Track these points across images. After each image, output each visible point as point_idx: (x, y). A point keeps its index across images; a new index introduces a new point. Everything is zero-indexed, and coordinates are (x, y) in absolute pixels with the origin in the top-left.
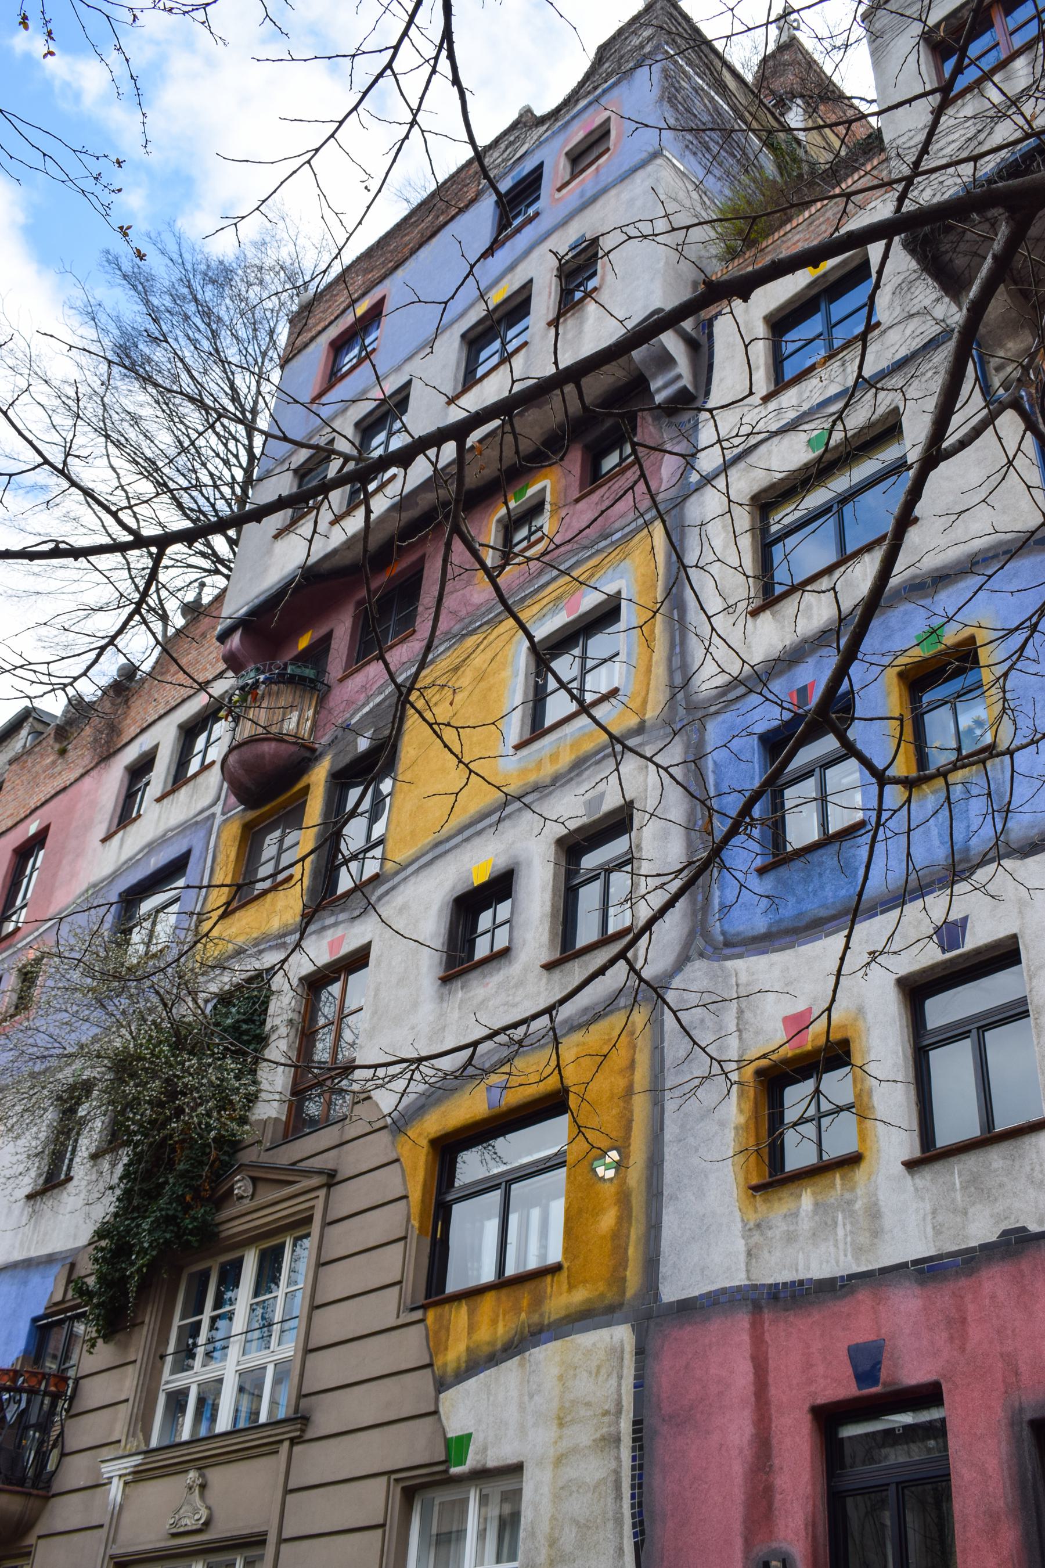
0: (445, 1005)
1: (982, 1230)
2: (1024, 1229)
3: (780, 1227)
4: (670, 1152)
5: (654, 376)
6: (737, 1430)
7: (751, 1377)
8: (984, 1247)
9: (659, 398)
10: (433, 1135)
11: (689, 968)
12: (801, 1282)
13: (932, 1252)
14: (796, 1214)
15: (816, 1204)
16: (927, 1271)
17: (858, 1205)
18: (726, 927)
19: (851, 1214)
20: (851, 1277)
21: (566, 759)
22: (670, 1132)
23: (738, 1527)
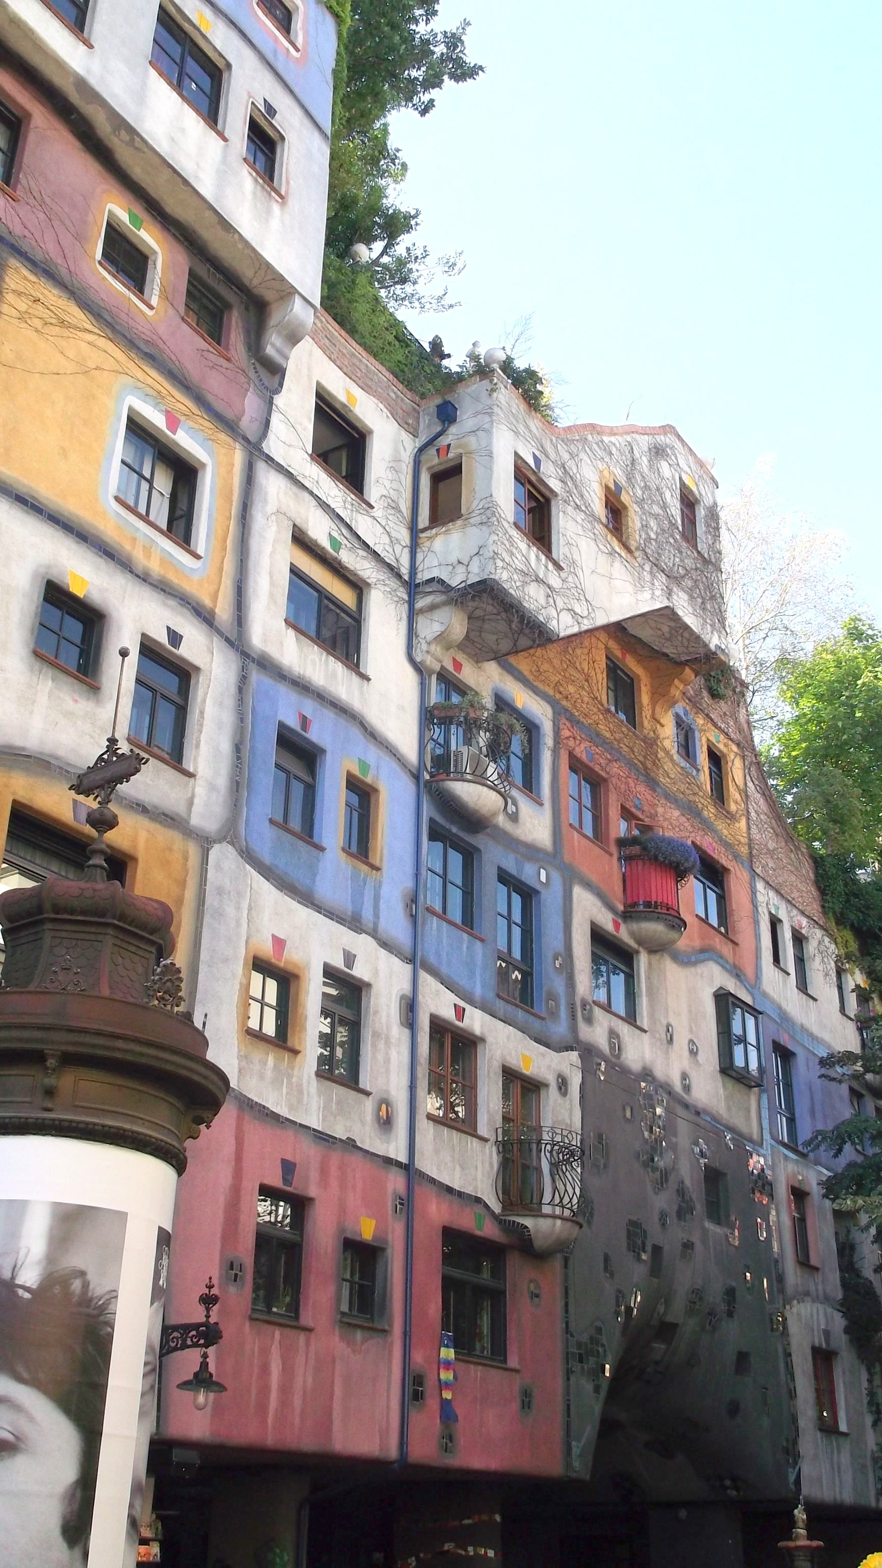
0: (35, 679)
1: (340, 1133)
2: (354, 1141)
3: (257, 1067)
4: (203, 969)
5: (279, 333)
6: (225, 1177)
7: (233, 1149)
8: (341, 1140)
9: (270, 351)
10: (18, 798)
11: (225, 844)
12: (264, 1107)
13: (320, 1129)
14: (265, 1063)
15: (275, 1065)
16: (321, 1137)
17: (294, 1080)
18: (248, 839)
19: (290, 1083)
20: (287, 1119)
21: (155, 567)
22: (204, 956)
23: (219, 1235)
